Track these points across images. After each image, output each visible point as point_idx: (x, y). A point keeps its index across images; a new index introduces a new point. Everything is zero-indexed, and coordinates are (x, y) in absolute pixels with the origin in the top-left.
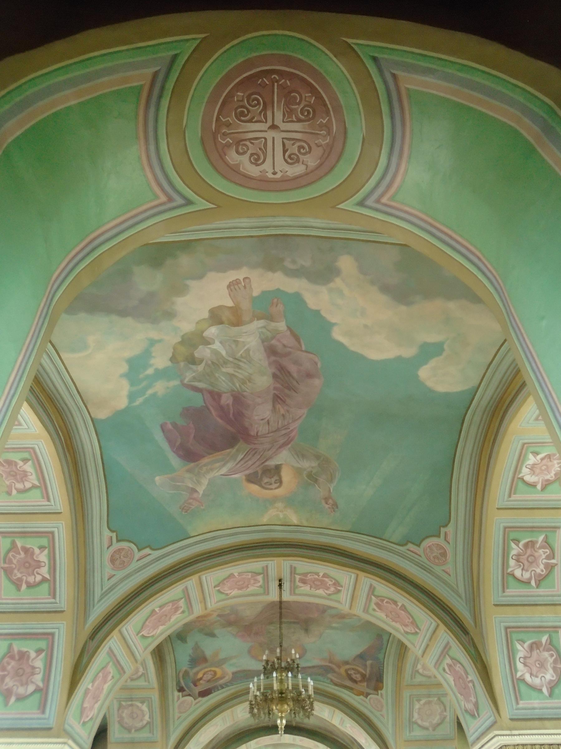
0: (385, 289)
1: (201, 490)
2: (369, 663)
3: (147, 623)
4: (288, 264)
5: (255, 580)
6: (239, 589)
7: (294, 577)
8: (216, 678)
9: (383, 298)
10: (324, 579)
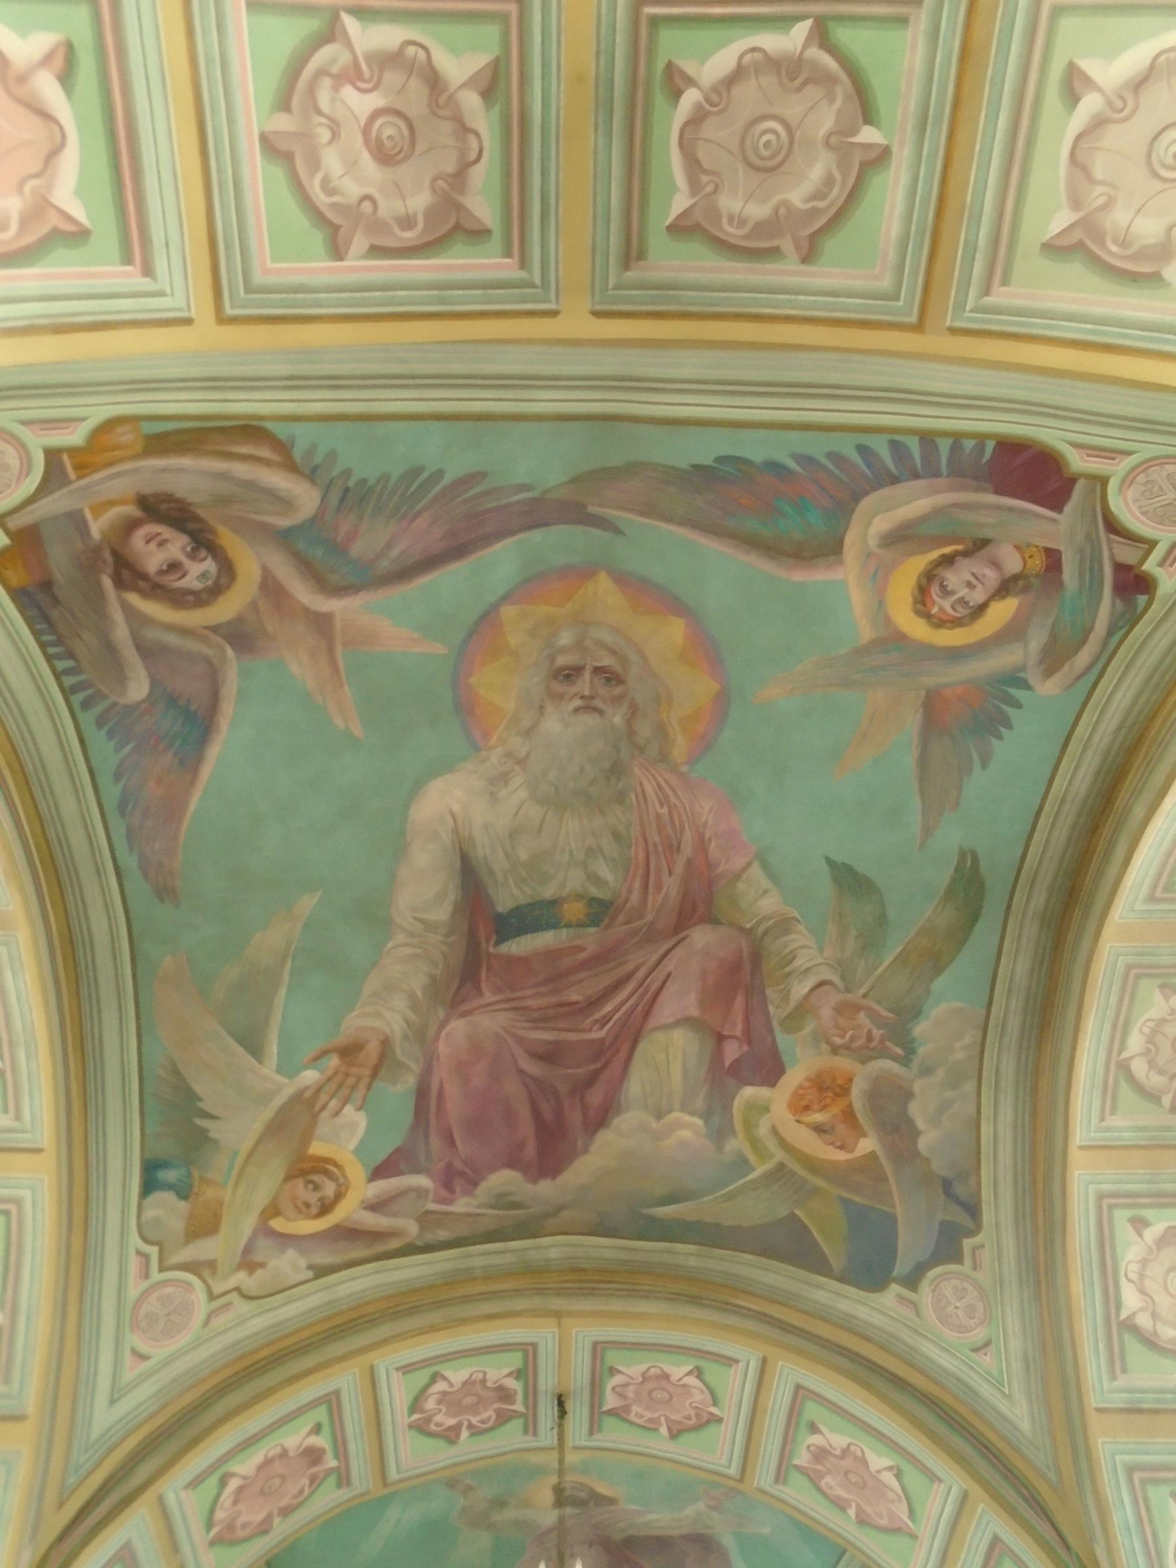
1: (701, 1506)
2: (138, 688)
3: (884, 1522)
5: (622, 1396)
6: (666, 1377)
7: (527, 1407)
8: (935, 555)
10: (451, 1422)
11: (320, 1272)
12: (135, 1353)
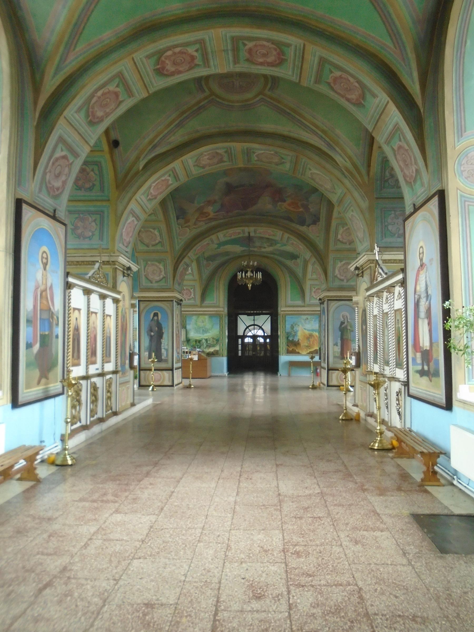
11: (206, 224)
12: (180, 239)
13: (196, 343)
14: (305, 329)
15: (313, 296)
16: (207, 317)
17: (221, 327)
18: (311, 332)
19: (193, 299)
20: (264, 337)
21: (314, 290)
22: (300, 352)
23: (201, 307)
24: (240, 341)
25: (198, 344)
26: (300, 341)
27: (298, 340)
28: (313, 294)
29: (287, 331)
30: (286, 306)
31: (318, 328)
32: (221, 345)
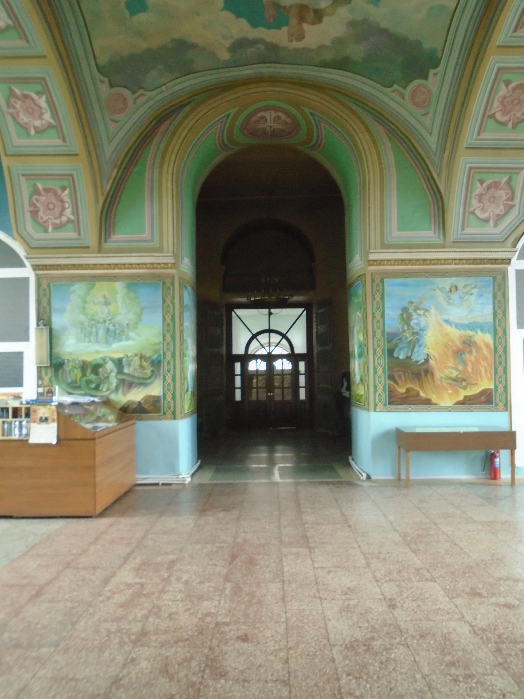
0: (194, 46)
4: (261, 46)
9: (193, 40)
13: (84, 375)
14: (447, 321)
15: (473, 213)
16: (119, 286)
17: (169, 320)
18: (471, 333)
19: (70, 226)
20: (293, 357)
21: (479, 189)
22: (434, 398)
23: (100, 250)
24: (238, 366)
25: (92, 377)
26: (432, 362)
27: (427, 361)
28: (474, 202)
29: (387, 330)
30: (385, 246)
31: (490, 319)
32: (169, 380)
